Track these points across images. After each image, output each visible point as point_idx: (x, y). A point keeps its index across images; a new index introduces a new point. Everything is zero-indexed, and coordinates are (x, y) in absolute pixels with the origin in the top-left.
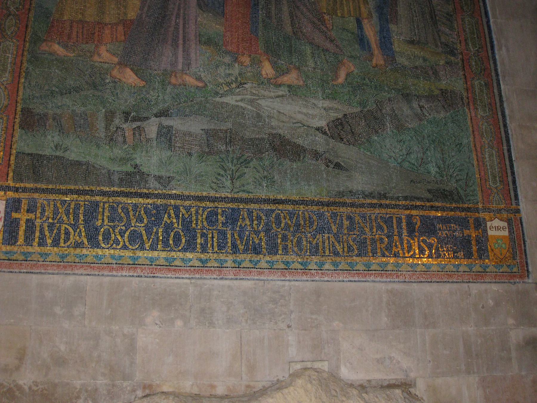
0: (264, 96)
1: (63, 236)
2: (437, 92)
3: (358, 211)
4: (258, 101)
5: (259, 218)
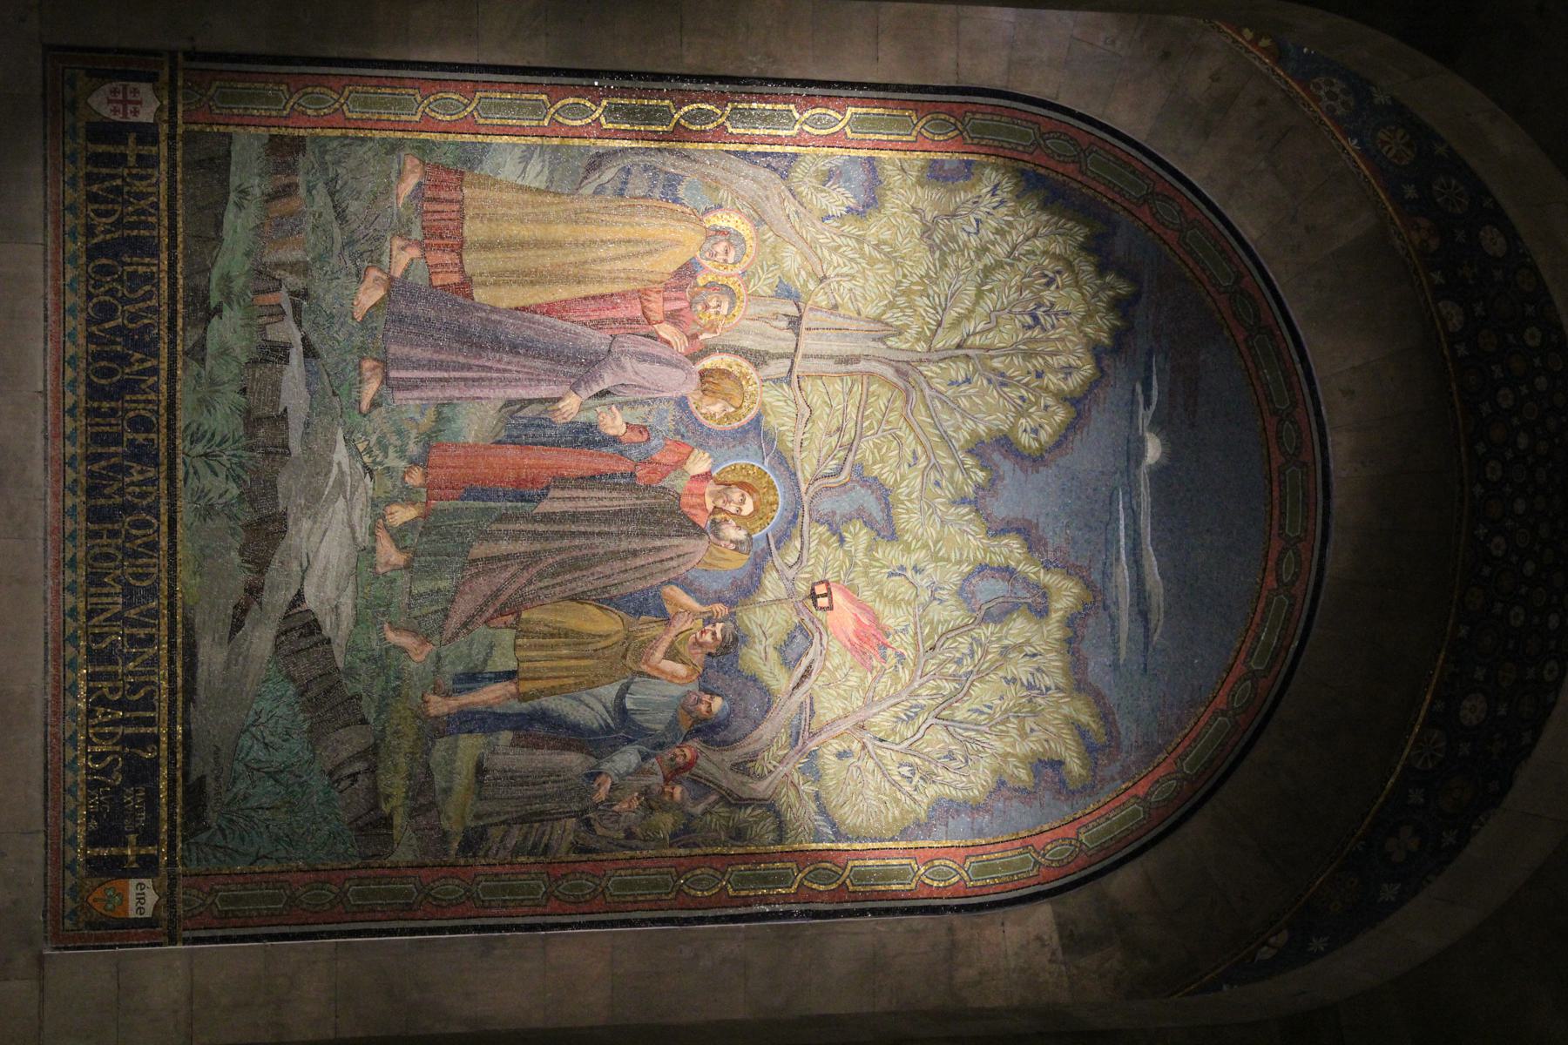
1: (103, 207)
2: (386, 808)
5: (143, 495)
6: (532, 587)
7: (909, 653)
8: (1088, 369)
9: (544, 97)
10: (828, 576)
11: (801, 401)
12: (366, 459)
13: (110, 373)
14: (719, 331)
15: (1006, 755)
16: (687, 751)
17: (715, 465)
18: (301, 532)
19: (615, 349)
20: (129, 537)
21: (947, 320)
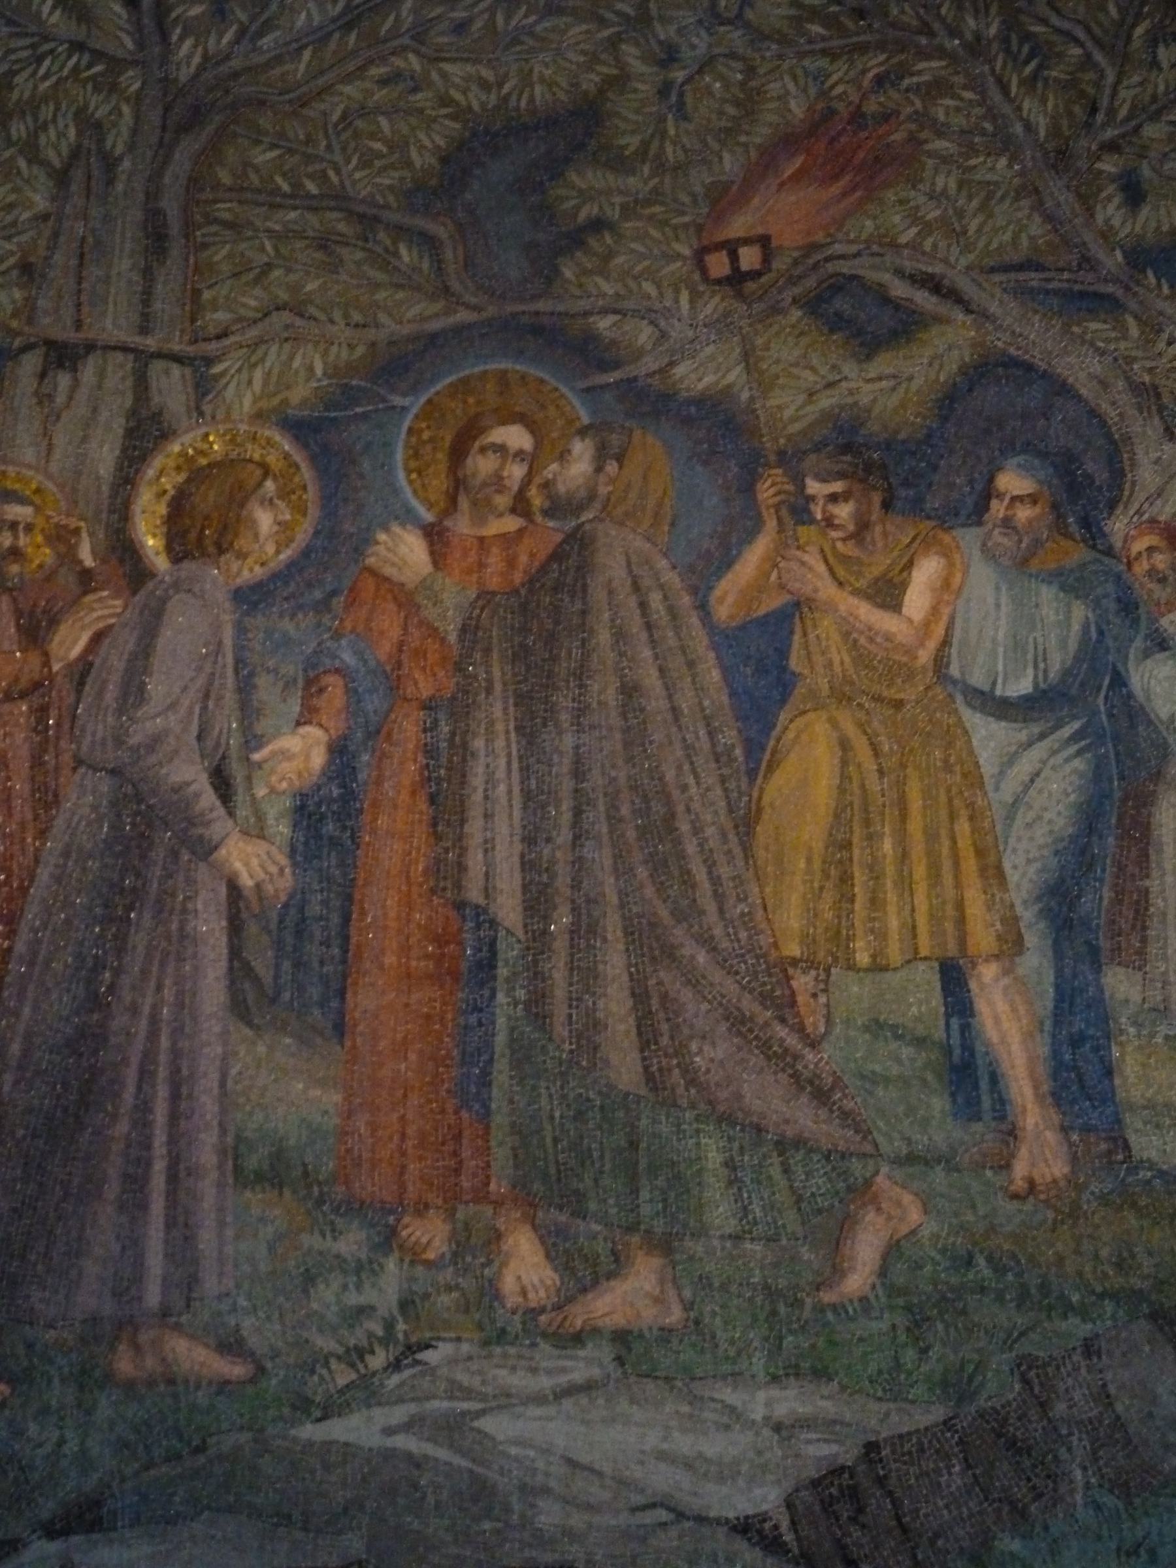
0: (508, 1396)
4: (487, 1424)
6: (718, 931)
7: (875, 63)
10: (686, 252)
12: (377, 1361)
14: (73, 523)
16: (1138, 546)
17: (407, 517)
21: (77, 32)
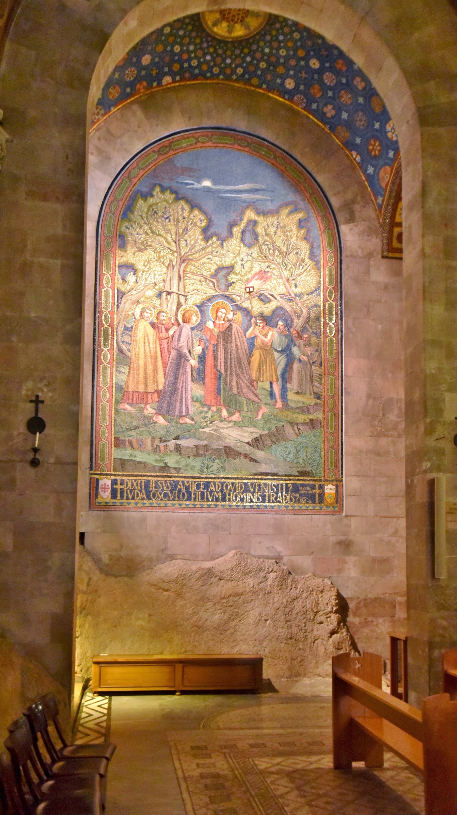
1: (136, 495)
2: (308, 421)
3: (263, 481)
7: (267, 264)
8: (182, 202)
9: (101, 366)
11: (192, 293)
12: (208, 423)
13: (183, 495)
15: (297, 237)
17: (211, 320)
18: (230, 442)
19: (176, 348)
20: (230, 490)
